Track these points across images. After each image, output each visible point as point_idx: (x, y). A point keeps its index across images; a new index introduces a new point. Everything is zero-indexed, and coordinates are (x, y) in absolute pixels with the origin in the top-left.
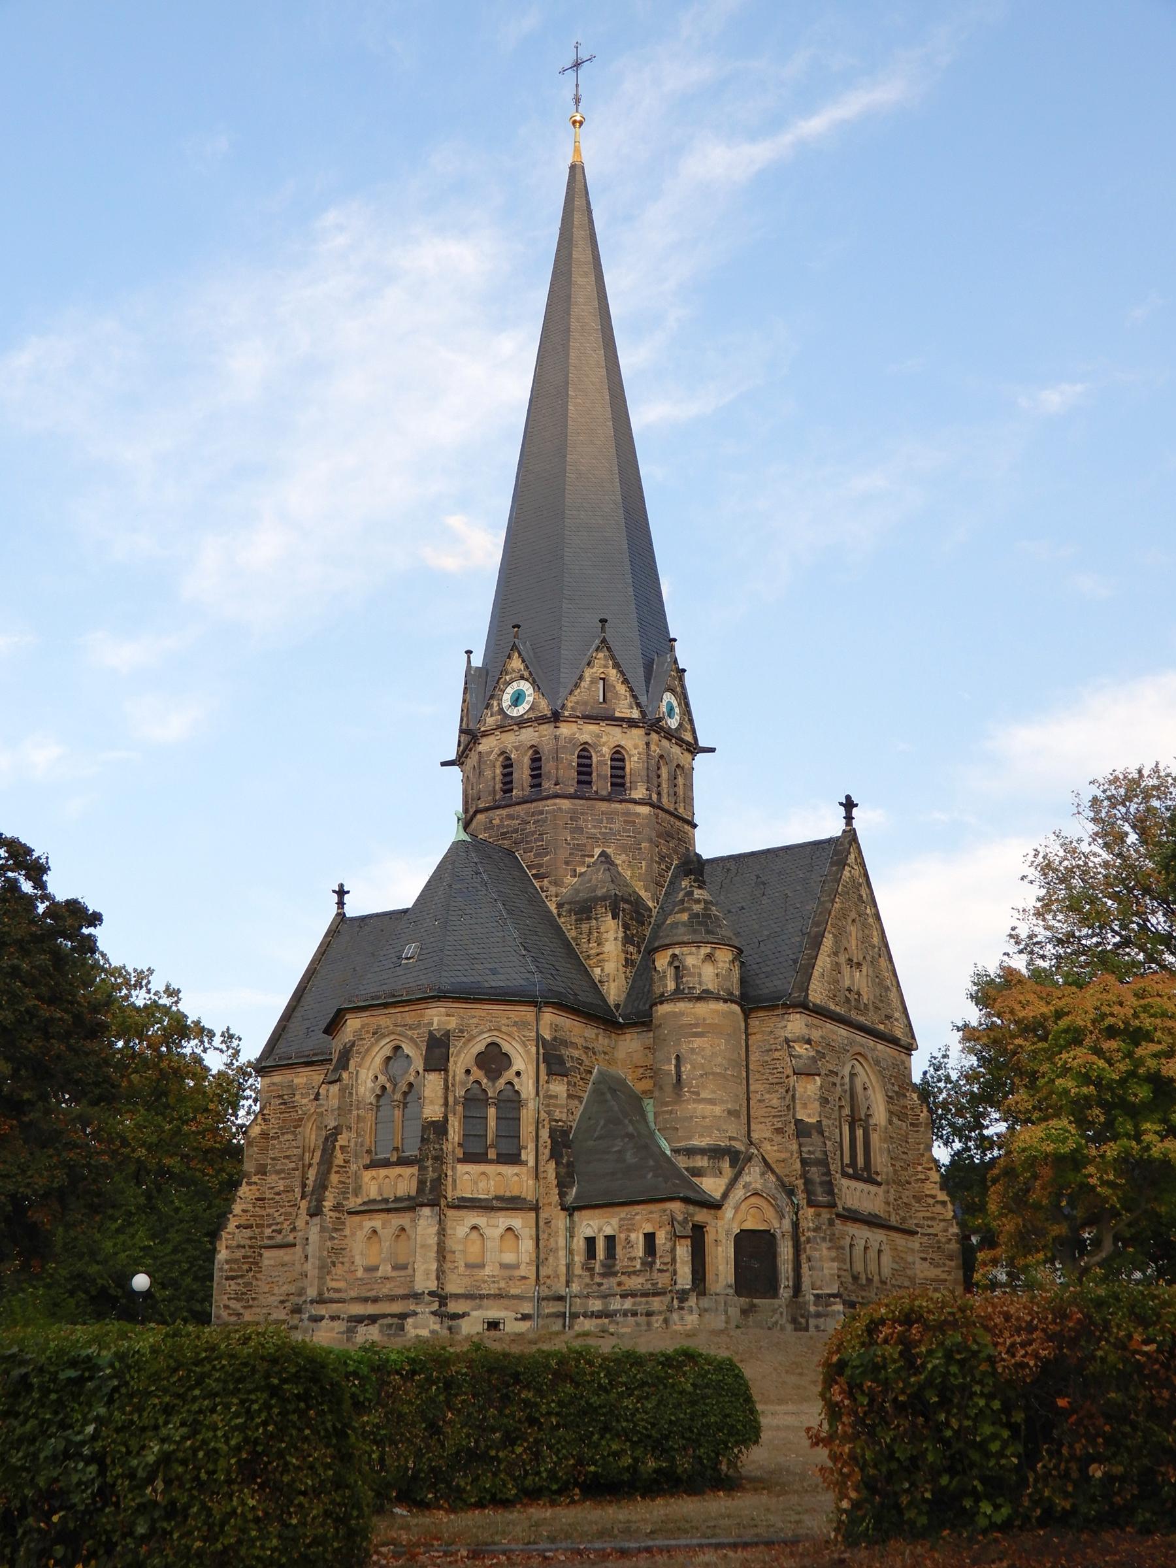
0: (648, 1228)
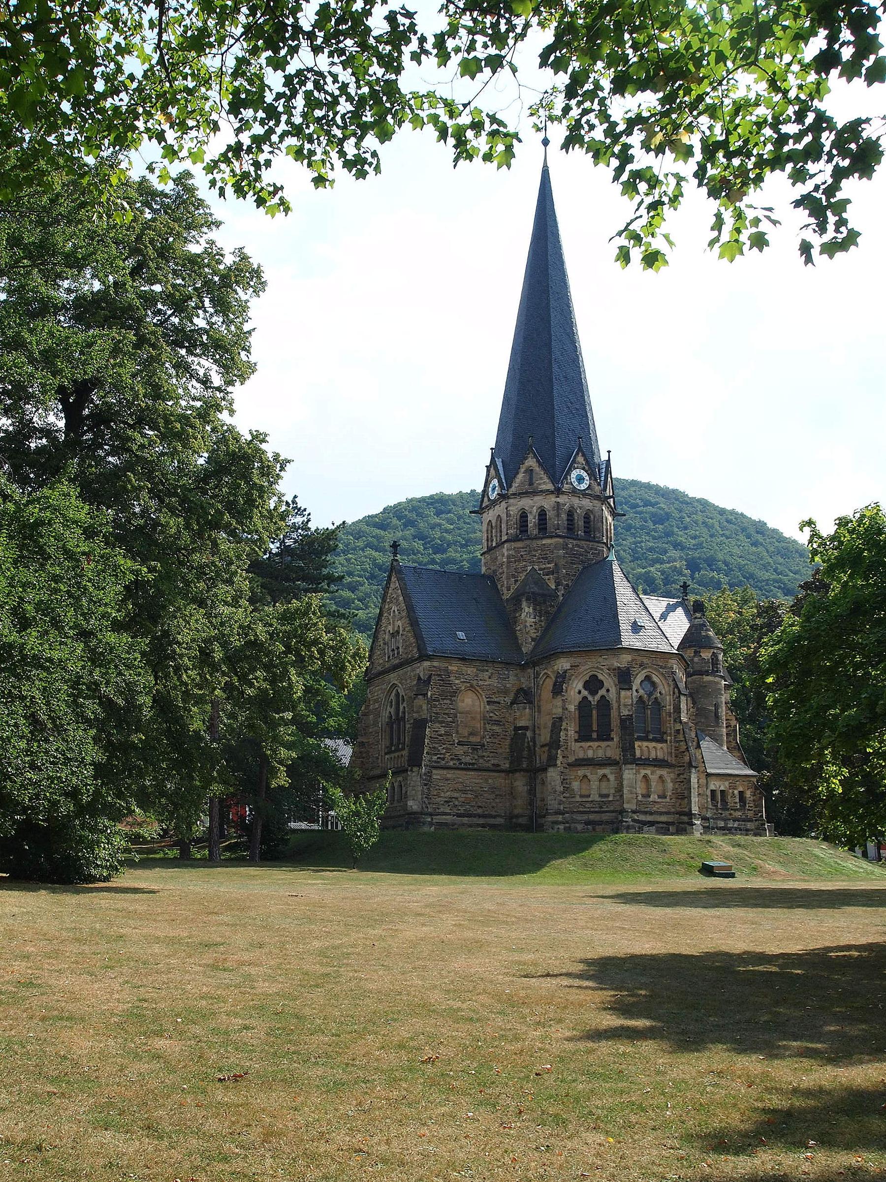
0: (741, 789)
